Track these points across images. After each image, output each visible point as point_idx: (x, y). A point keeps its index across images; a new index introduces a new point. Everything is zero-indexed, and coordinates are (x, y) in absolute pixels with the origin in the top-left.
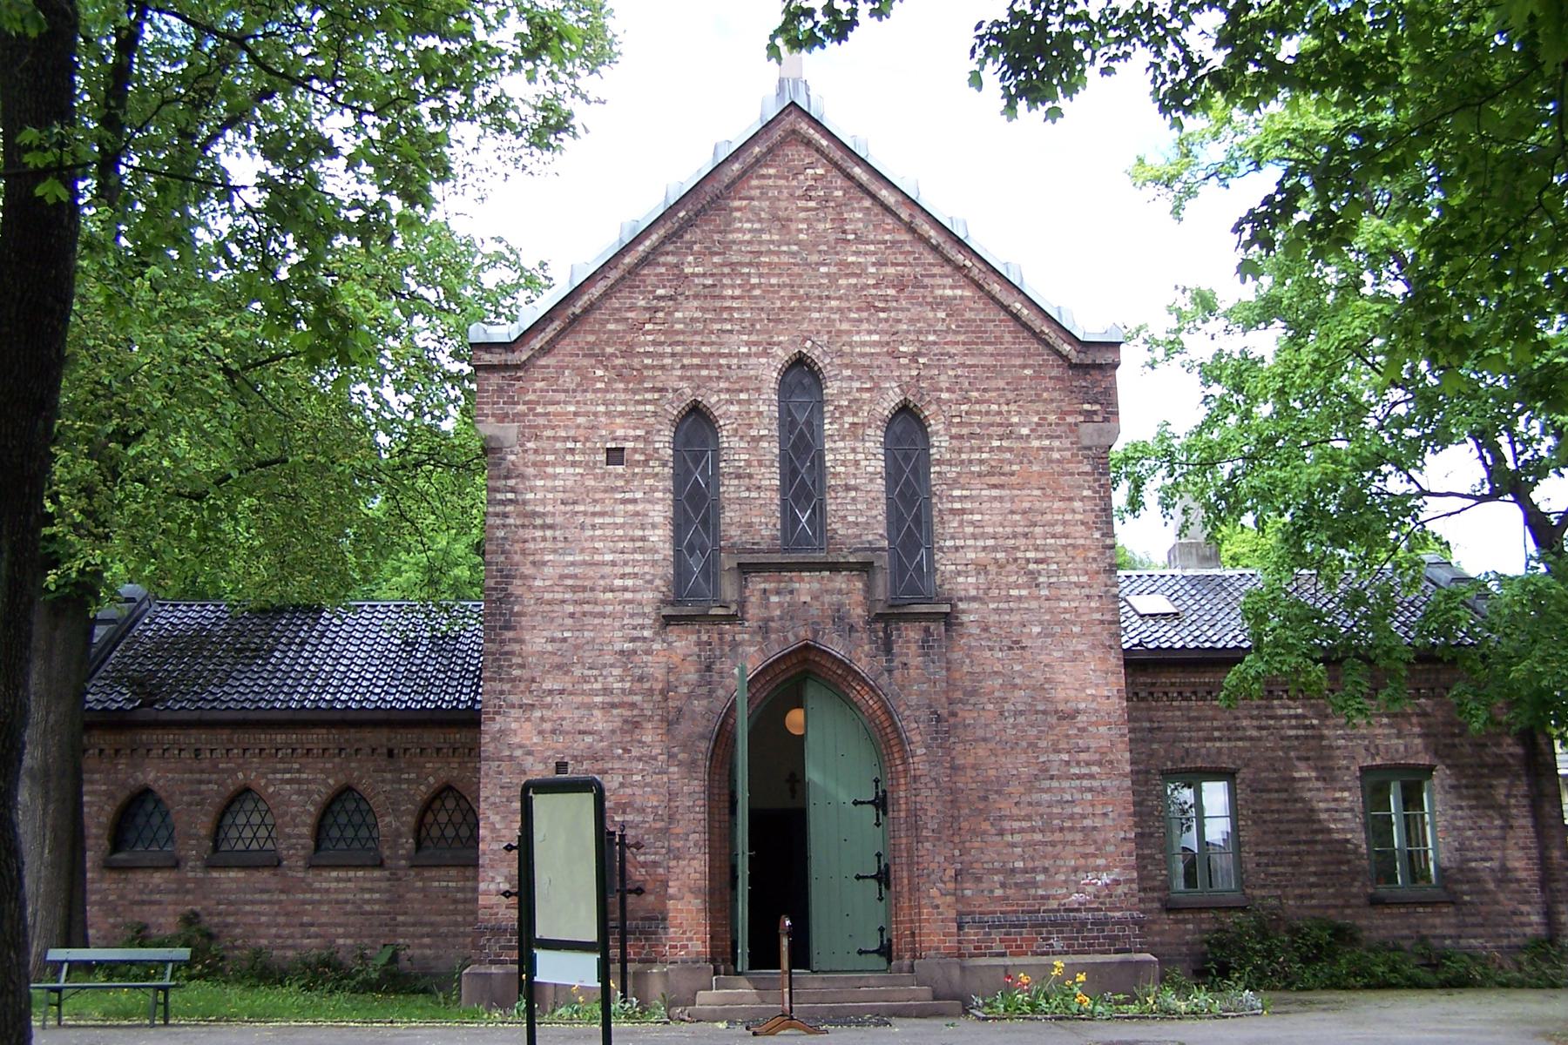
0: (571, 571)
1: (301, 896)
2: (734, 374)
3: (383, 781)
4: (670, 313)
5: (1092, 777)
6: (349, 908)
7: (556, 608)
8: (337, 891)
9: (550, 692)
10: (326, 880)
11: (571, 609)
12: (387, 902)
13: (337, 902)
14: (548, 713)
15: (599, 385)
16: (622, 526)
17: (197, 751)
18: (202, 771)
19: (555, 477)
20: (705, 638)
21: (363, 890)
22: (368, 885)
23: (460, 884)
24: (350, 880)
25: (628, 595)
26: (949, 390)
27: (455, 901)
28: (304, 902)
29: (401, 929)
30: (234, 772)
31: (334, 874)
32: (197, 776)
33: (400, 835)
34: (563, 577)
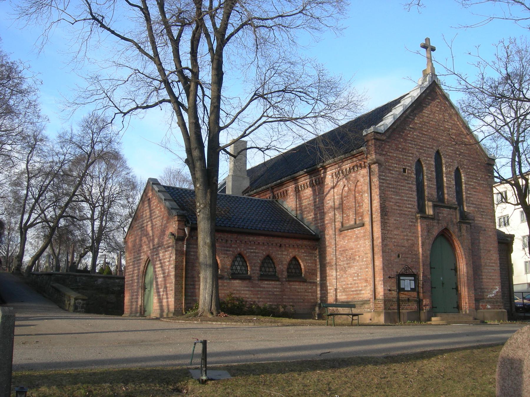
0: (398, 201)
1: (257, 289)
2: (427, 152)
3: (278, 254)
4: (413, 133)
5: (493, 266)
6: (270, 293)
7: (396, 211)
8: (267, 288)
9: (396, 235)
10: (264, 284)
11: (398, 212)
12: (281, 292)
13: (267, 291)
14: (396, 240)
15: (400, 150)
16: (407, 190)
17: (227, 241)
18: (227, 247)
19: (393, 174)
20: (427, 223)
21: (274, 288)
22: (275, 286)
23: (299, 287)
24: (270, 284)
25: (410, 210)
26: (466, 165)
27: (298, 292)
28: (258, 291)
29: (284, 300)
30: (236, 248)
31: (266, 282)
32: (226, 249)
33: (283, 271)
34: (396, 203)
